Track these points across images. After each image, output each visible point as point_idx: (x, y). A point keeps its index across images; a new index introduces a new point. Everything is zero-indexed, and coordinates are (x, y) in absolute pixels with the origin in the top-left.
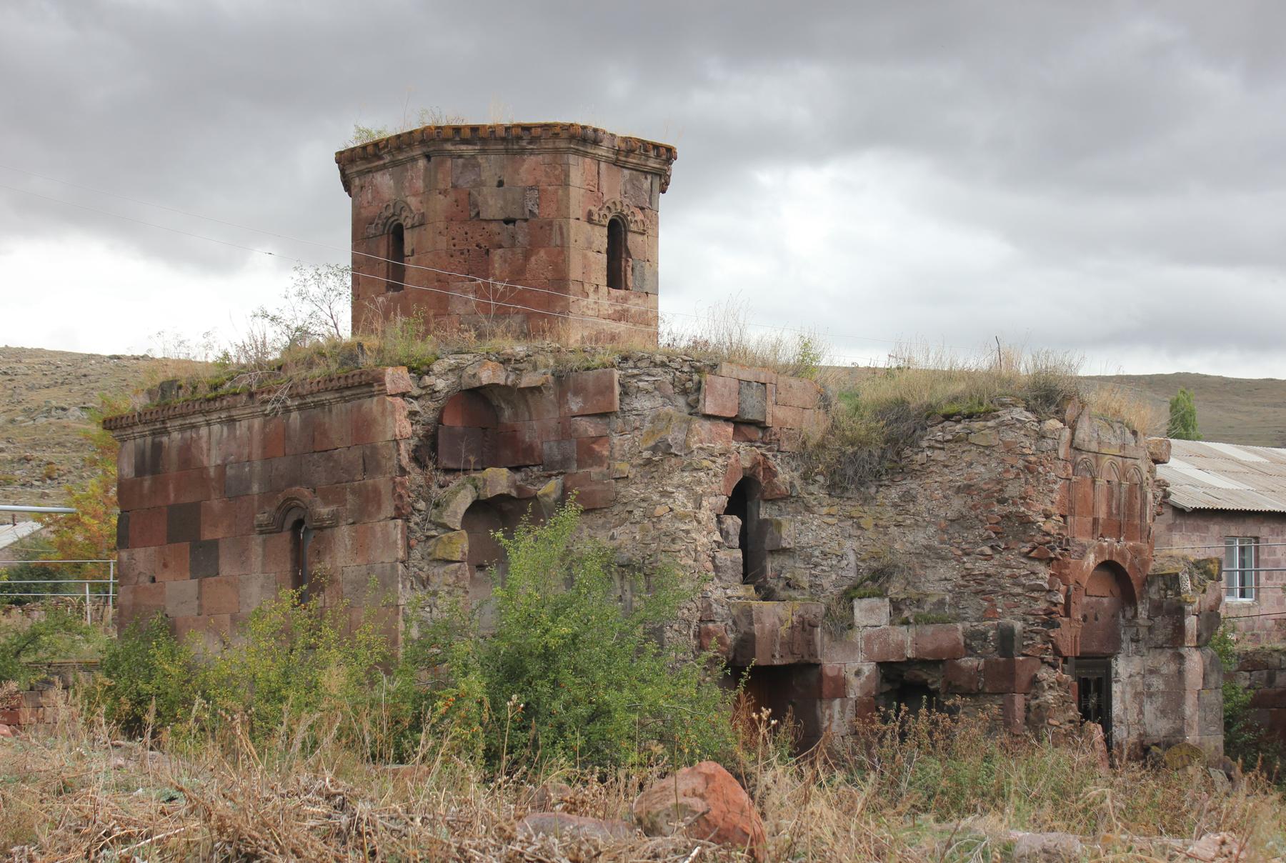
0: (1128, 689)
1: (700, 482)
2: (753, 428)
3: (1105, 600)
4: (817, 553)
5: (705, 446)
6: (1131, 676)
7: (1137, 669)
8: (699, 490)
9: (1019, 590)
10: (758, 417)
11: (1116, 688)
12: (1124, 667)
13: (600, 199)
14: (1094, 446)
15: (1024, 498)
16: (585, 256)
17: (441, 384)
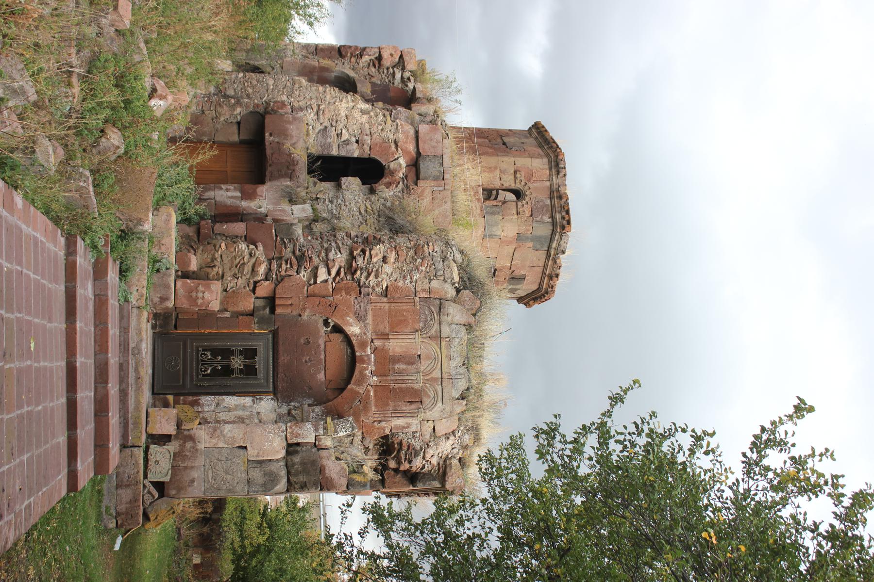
0: (247, 413)
1: (376, 116)
2: (415, 179)
3: (321, 376)
4: (340, 201)
5: (399, 127)
6: (258, 413)
7: (264, 418)
8: (372, 114)
9: (326, 246)
10: (422, 175)
11: (248, 400)
12: (267, 406)
13: (529, 181)
14: (446, 330)
15: (395, 247)
16: (496, 168)
17: (411, 86)
